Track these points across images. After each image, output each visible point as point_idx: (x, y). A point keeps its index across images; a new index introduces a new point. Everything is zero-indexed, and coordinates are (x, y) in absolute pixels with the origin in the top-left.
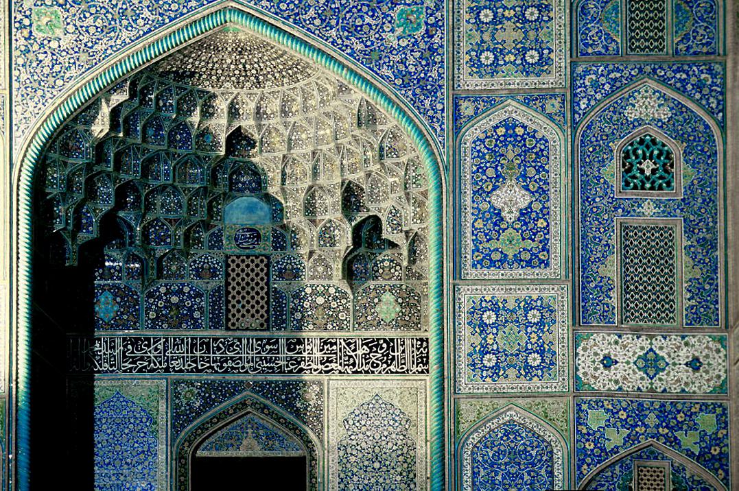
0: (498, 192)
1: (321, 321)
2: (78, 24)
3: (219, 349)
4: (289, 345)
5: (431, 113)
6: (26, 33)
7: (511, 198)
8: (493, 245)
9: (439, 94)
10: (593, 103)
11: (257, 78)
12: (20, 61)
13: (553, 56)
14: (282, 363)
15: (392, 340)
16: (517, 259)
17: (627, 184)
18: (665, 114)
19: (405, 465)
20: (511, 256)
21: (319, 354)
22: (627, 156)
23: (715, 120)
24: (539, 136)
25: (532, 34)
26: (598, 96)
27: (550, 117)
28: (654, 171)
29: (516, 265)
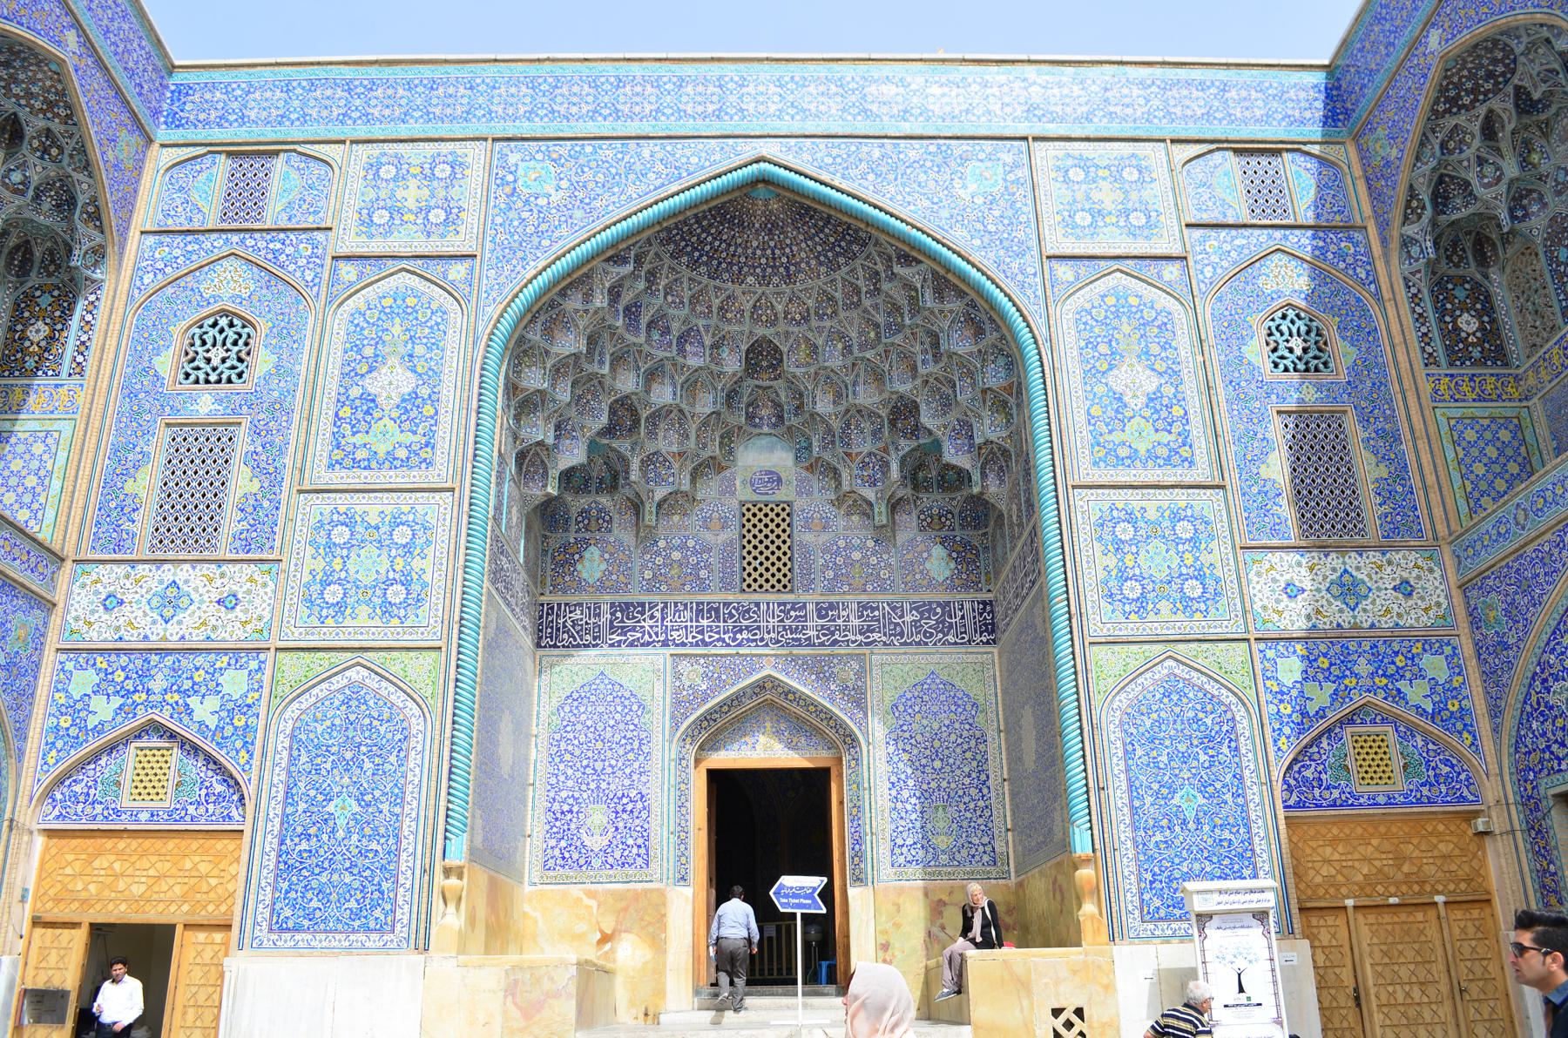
0: (1115, 372)
1: (858, 582)
2: (574, 179)
5: (1020, 277)
6: (508, 190)
7: (1135, 380)
8: (1117, 437)
9: (1028, 256)
10: (1219, 271)
11: (787, 269)
12: (499, 220)
14: (811, 633)
16: (1152, 456)
17: (1276, 365)
19: (974, 764)
20: (1142, 451)
21: (856, 622)
22: (1270, 334)
23: (1370, 292)
24: (1158, 306)
28: (1305, 350)
29: (1150, 463)
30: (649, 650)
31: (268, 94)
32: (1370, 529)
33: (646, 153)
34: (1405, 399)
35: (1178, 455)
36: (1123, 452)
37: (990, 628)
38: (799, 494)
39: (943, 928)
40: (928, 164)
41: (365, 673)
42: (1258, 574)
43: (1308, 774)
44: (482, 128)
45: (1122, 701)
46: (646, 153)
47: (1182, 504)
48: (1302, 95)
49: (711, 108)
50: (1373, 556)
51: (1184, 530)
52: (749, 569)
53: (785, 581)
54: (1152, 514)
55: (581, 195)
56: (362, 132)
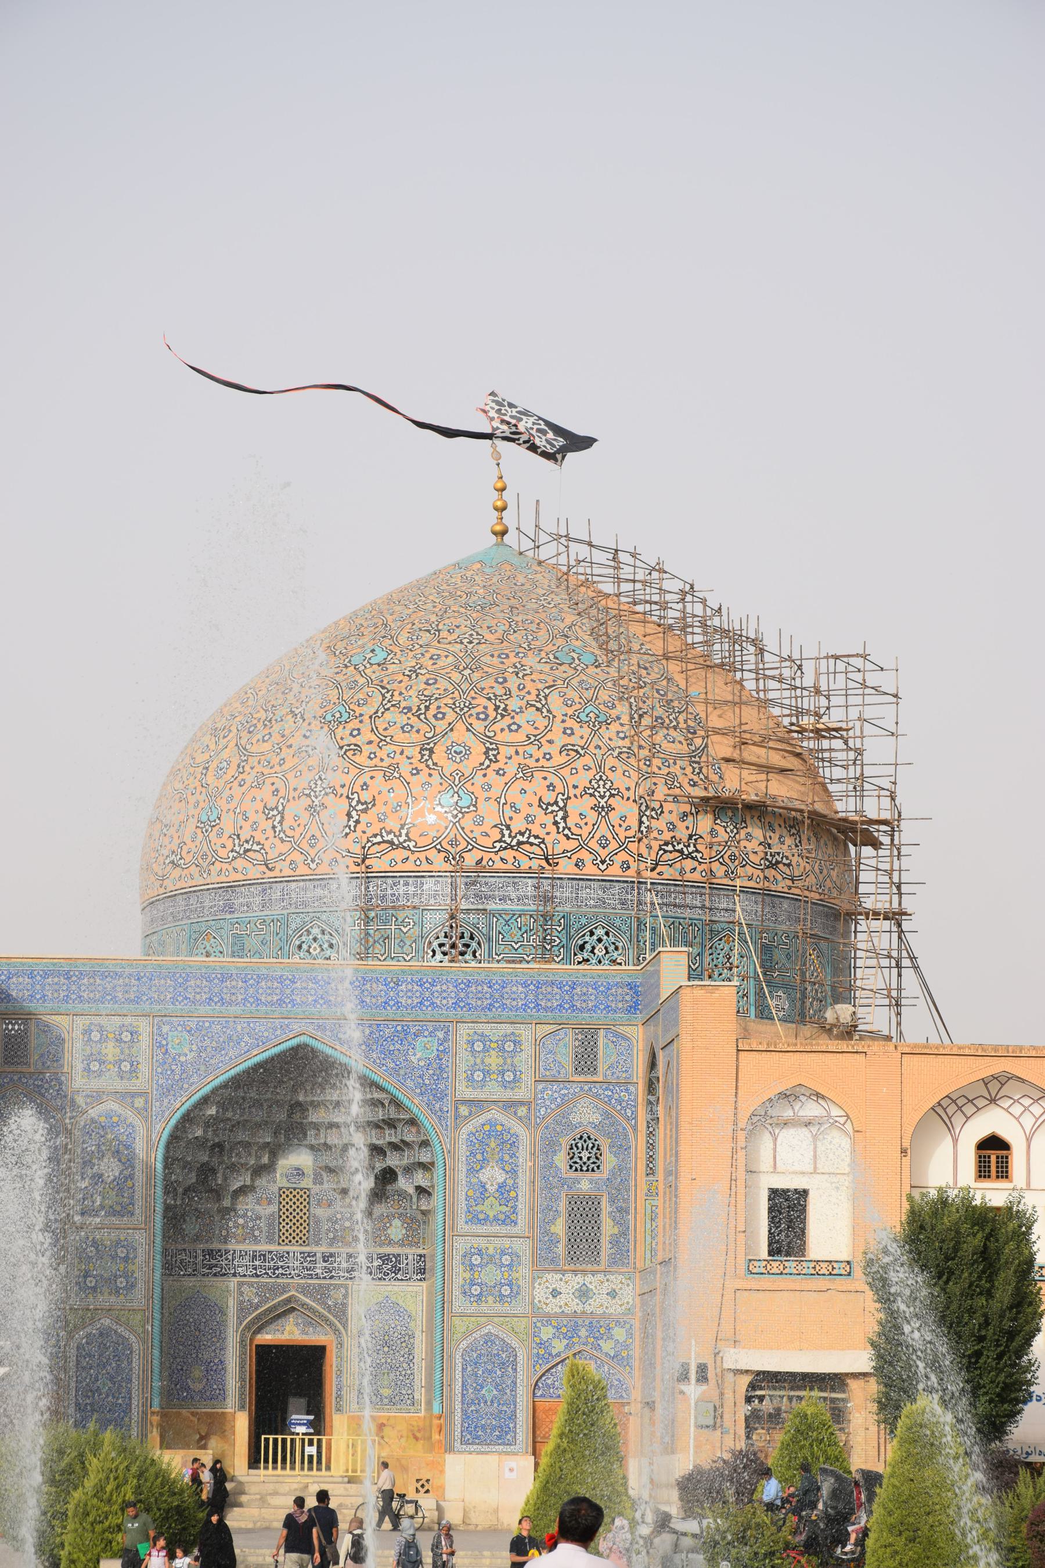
3: (273, 1259)
4: (324, 1257)
5: (439, 1113)
6: (163, 1050)
7: (493, 1175)
8: (479, 1208)
12: (159, 1070)
13: (523, 1076)
14: (319, 1271)
15: (399, 1255)
16: (496, 1219)
17: (571, 1167)
18: (596, 1118)
22: (571, 1148)
25: (509, 1061)
26: (553, 1106)
27: (520, 1118)
28: (589, 1158)
30: (224, 1278)
31: (21, 979)
32: (603, 1262)
33: (239, 1028)
34: (636, 1191)
35: (509, 1220)
36: (481, 1216)
37: (422, 1271)
38: (315, 1183)
39: (382, 1437)
40: (396, 1039)
41: (108, 1321)
42: (540, 1284)
43: (549, 1382)
44: (146, 1007)
45: (464, 1344)
46: (239, 1028)
47: (507, 1246)
48: (620, 991)
49: (275, 998)
50: (600, 1277)
51: (506, 1260)
52: (284, 1230)
53: (304, 1238)
54: (491, 1251)
55: (203, 1055)
56: (79, 1007)
